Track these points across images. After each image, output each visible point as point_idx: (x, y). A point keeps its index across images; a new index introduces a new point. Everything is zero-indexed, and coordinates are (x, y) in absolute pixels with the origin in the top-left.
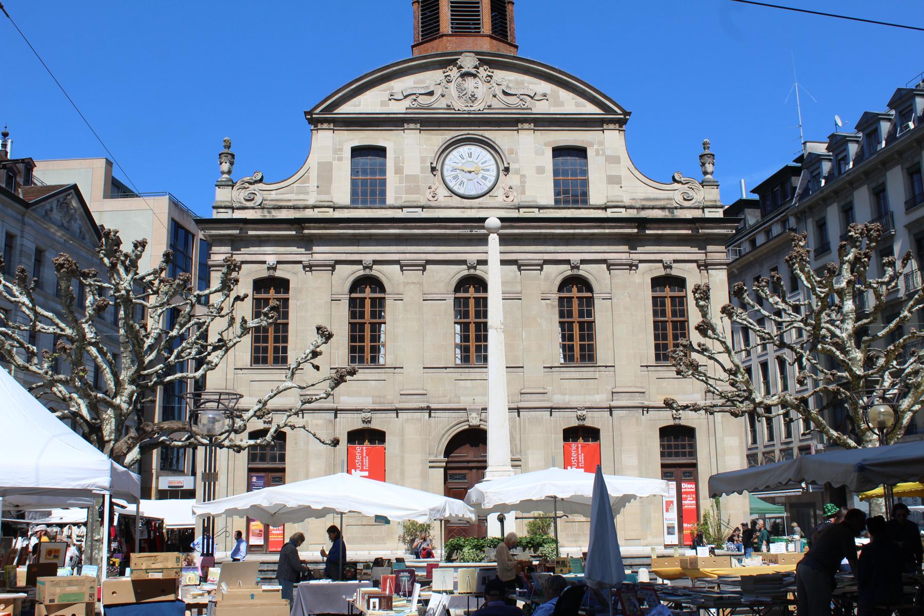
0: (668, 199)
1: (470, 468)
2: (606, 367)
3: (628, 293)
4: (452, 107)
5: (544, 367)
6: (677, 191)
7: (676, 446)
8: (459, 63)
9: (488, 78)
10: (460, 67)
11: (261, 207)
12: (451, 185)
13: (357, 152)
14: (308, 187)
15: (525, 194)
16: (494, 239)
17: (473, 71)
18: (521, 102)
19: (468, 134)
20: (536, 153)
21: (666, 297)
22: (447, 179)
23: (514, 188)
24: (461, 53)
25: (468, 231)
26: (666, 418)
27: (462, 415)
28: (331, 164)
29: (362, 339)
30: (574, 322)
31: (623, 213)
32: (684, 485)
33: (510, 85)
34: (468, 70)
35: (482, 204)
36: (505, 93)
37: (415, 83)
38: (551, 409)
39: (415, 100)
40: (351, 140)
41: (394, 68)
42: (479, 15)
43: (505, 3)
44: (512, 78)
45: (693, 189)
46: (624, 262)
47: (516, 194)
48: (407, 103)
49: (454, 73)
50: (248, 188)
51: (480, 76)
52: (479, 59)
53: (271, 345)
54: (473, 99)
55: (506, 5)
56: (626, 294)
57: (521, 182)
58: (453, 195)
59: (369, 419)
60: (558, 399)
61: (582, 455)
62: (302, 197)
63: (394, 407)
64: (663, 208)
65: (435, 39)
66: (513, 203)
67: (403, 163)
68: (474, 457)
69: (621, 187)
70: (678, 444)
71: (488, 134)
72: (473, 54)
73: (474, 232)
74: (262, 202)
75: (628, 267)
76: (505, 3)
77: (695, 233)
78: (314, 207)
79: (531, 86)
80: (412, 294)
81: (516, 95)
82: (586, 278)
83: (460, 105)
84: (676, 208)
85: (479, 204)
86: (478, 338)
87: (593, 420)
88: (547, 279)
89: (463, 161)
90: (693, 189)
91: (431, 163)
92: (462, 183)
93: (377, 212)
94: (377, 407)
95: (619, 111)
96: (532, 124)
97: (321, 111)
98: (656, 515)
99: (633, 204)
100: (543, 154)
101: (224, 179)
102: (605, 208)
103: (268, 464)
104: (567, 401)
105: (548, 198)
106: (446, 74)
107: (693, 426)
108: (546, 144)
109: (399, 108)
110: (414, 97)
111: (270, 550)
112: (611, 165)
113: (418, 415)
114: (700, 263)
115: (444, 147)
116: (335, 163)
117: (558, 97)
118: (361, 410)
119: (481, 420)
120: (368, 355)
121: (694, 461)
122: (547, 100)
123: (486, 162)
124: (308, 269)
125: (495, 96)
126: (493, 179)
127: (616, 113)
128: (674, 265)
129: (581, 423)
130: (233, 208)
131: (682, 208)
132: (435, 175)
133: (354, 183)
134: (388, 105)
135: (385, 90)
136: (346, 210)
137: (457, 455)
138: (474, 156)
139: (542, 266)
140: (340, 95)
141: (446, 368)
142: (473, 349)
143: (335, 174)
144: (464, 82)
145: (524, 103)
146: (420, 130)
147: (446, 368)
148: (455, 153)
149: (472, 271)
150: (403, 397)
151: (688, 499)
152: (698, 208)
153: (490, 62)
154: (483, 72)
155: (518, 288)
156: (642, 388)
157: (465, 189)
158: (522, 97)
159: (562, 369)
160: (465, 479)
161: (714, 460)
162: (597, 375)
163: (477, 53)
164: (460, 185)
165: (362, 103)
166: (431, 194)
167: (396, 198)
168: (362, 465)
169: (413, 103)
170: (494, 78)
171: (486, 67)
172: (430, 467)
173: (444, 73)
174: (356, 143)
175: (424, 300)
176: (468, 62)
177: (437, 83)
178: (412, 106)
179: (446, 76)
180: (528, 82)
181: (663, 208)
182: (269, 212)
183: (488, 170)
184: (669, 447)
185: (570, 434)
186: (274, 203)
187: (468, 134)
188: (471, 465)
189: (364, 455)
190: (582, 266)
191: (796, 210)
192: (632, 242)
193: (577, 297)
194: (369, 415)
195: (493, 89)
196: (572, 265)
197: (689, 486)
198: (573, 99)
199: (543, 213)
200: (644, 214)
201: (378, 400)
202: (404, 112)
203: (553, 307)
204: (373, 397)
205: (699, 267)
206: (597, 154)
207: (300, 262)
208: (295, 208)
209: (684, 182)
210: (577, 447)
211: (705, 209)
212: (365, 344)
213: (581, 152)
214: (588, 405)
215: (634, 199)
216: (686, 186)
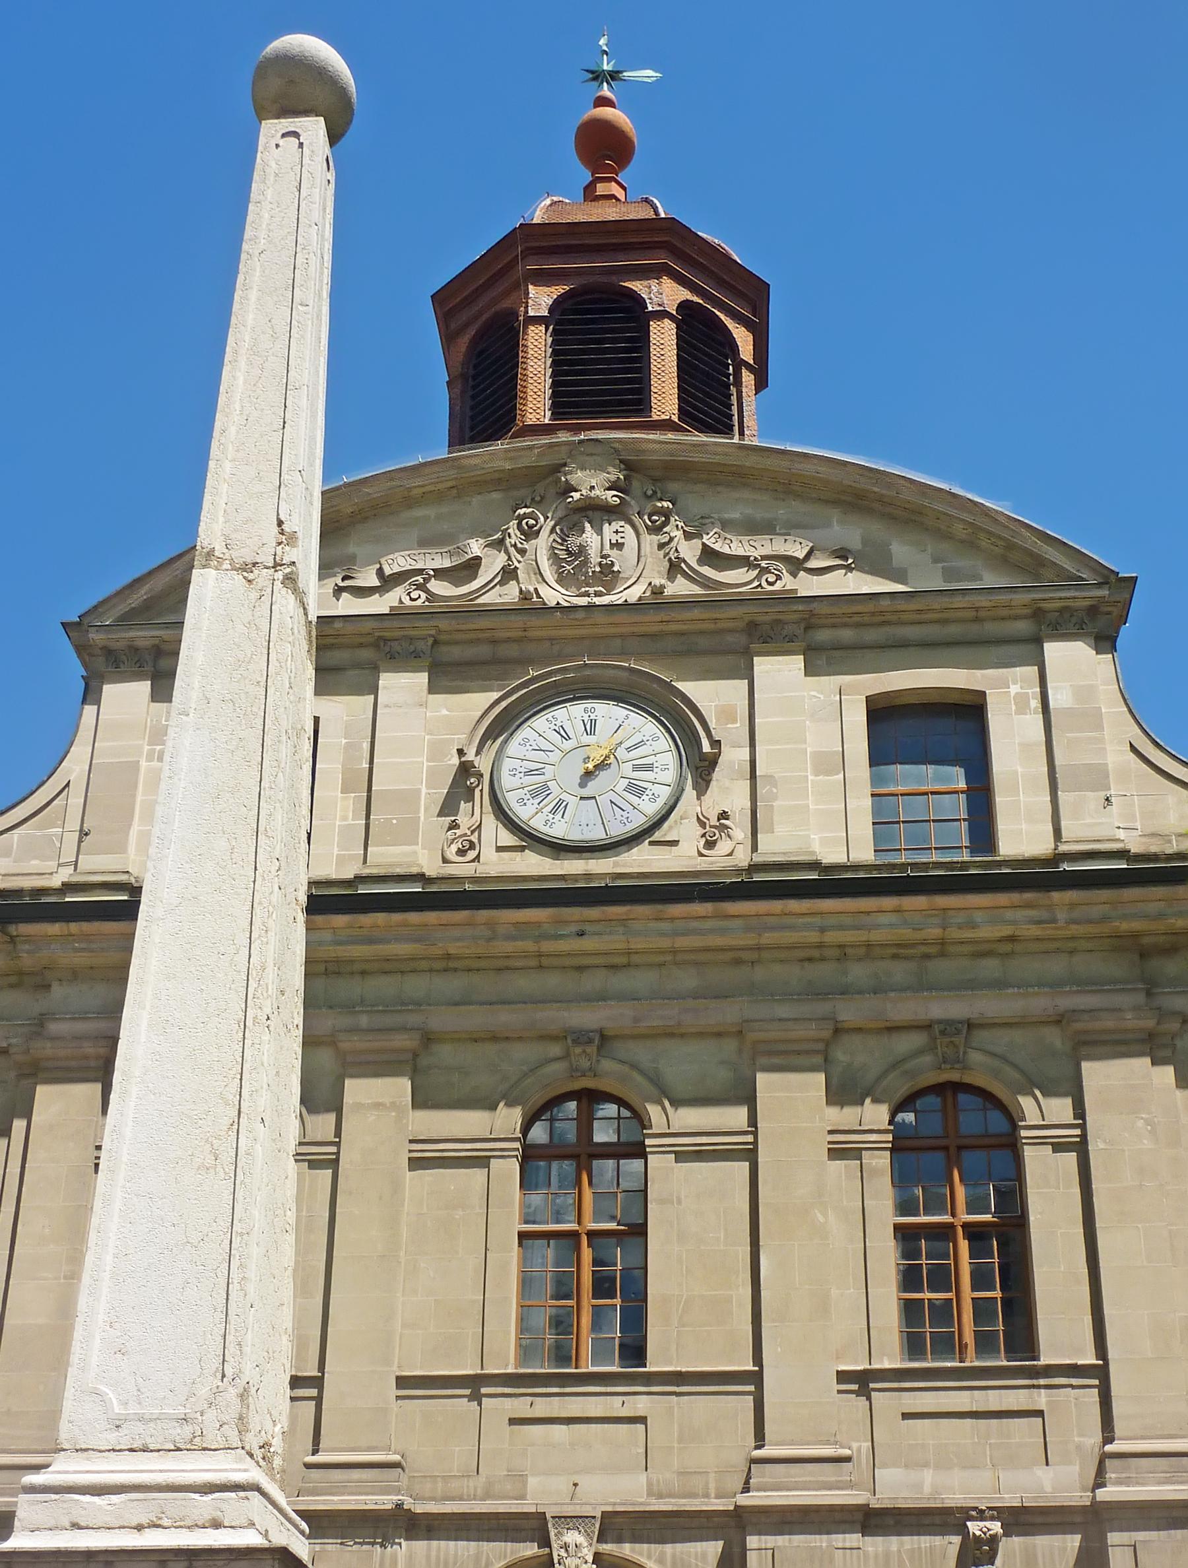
3: (1148, 1122)
15: (773, 832)
22: (512, 800)
56: (1140, 1123)
89: (567, 745)
91: (461, 752)
104: (927, 1490)
126: (664, 793)
158: (764, 564)
162: (1041, 1399)
164: (554, 811)
169: (414, 595)
195: (673, 544)
215: (1153, 835)
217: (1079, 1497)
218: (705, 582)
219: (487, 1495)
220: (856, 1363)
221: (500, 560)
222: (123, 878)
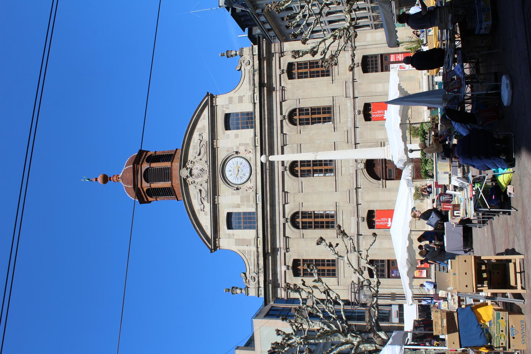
0: (249, 72)
1: (386, 167)
2: (333, 101)
3: (296, 91)
4: (207, 180)
5: (334, 132)
7: (372, 64)
8: (185, 177)
9: (192, 163)
10: (187, 177)
11: (258, 273)
12: (245, 180)
13: (230, 227)
14: (247, 250)
15: (248, 144)
16: (271, 158)
17: (189, 170)
18: (204, 147)
19: (220, 172)
20: (228, 138)
21: (298, 72)
22: (242, 182)
23: (246, 149)
24: (180, 177)
25: (268, 171)
26: (358, 70)
27: (359, 172)
28: (236, 239)
29: (322, 223)
30: (311, 117)
31: (257, 94)
32: (392, 60)
33: (195, 152)
34: (189, 173)
36: (199, 154)
37: (195, 199)
38: (355, 127)
39: (204, 199)
41: (189, 209)
42: (162, 168)
43: (156, 156)
44: (192, 151)
45: (244, 61)
46: (281, 93)
47: (249, 148)
48: (205, 202)
49: (190, 180)
50: (248, 280)
51: (191, 167)
52: (183, 167)
53: (326, 268)
54: (202, 170)
55: (156, 155)
57: (243, 145)
59: (362, 218)
60: (350, 125)
61: (378, 111)
62: (252, 253)
63: (356, 206)
64: (254, 75)
65: (174, 189)
68: (380, 165)
69: (244, 96)
70: (371, 64)
71: (220, 163)
72: (181, 171)
73: (268, 168)
74: (255, 273)
75: (283, 91)
76: (156, 156)
77: (266, 59)
78: (257, 247)
79: (196, 142)
80: (300, 198)
81: (200, 149)
82: (289, 112)
83: (206, 177)
84: (254, 68)
85: (254, 166)
86: (321, 165)
87: (360, 107)
88: (290, 131)
89: (233, 174)
90: (244, 61)
91: (235, 190)
92: (244, 175)
93: (259, 216)
94: (356, 214)
96: (214, 141)
97: (210, 245)
98: (407, 73)
99: (252, 90)
100: (228, 135)
101: (245, 292)
102: (255, 103)
103: (385, 268)
104: (351, 120)
105: (249, 133)
106: (191, 184)
108: (224, 133)
109: (208, 207)
110: (202, 199)
111: (429, 266)
112: (233, 101)
113: (360, 194)
114: (280, 56)
115: (226, 184)
116: (235, 237)
118: (358, 222)
119: (362, 163)
120: (330, 220)
121: (379, 55)
122: (202, 134)
123: (233, 163)
124: (288, 250)
125: (201, 160)
126: (242, 159)
128: (282, 68)
129: (362, 112)
130: (259, 287)
132: (240, 188)
133: (245, 228)
135: (199, 213)
136: (259, 232)
137: (379, 174)
139: (284, 134)
140: (202, 235)
141: (336, 181)
142: (326, 167)
144: (194, 175)
145: (204, 145)
146: (218, 196)
147: (336, 181)
148: (229, 179)
149: (287, 169)
151: (398, 58)
152: (253, 57)
154: (189, 166)
155: (295, 145)
156: (343, 83)
157: (247, 173)
158: (201, 146)
160: (391, 170)
161: (379, 46)
162: (338, 105)
163: (180, 169)
164: (245, 175)
166: (250, 189)
167: (252, 207)
168: (385, 221)
169: (205, 199)
171: (187, 164)
172: (386, 187)
173: (190, 185)
174: (226, 227)
175: (302, 192)
176: (185, 173)
177: (195, 188)
178: (207, 200)
179: (192, 184)
180: (194, 143)
181: (254, 75)
182: (260, 269)
183: (237, 162)
184: (372, 68)
185: (367, 117)
186: (256, 267)
187: (220, 172)
188: (384, 167)
189: (380, 220)
190: (284, 114)
191: (253, 9)
192: (271, 90)
193: (299, 116)
194: (360, 218)
195: (197, 160)
196: (283, 119)
197: (392, 57)
198: (201, 121)
199: (258, 134)
203: (304, 128)
204: (351, 216)
205: (282, 56)
206: (228, 108)
207: (285, 254)
208: (258, 257)
209: (241, 65)
210: (374, 114)
211: (254, 54)
212: (325, 221)
213: (227, 117)
214: (352, 109)
216: (242, 64)
218: (204, 155)
220: (333, 130)
222: (255, 239)
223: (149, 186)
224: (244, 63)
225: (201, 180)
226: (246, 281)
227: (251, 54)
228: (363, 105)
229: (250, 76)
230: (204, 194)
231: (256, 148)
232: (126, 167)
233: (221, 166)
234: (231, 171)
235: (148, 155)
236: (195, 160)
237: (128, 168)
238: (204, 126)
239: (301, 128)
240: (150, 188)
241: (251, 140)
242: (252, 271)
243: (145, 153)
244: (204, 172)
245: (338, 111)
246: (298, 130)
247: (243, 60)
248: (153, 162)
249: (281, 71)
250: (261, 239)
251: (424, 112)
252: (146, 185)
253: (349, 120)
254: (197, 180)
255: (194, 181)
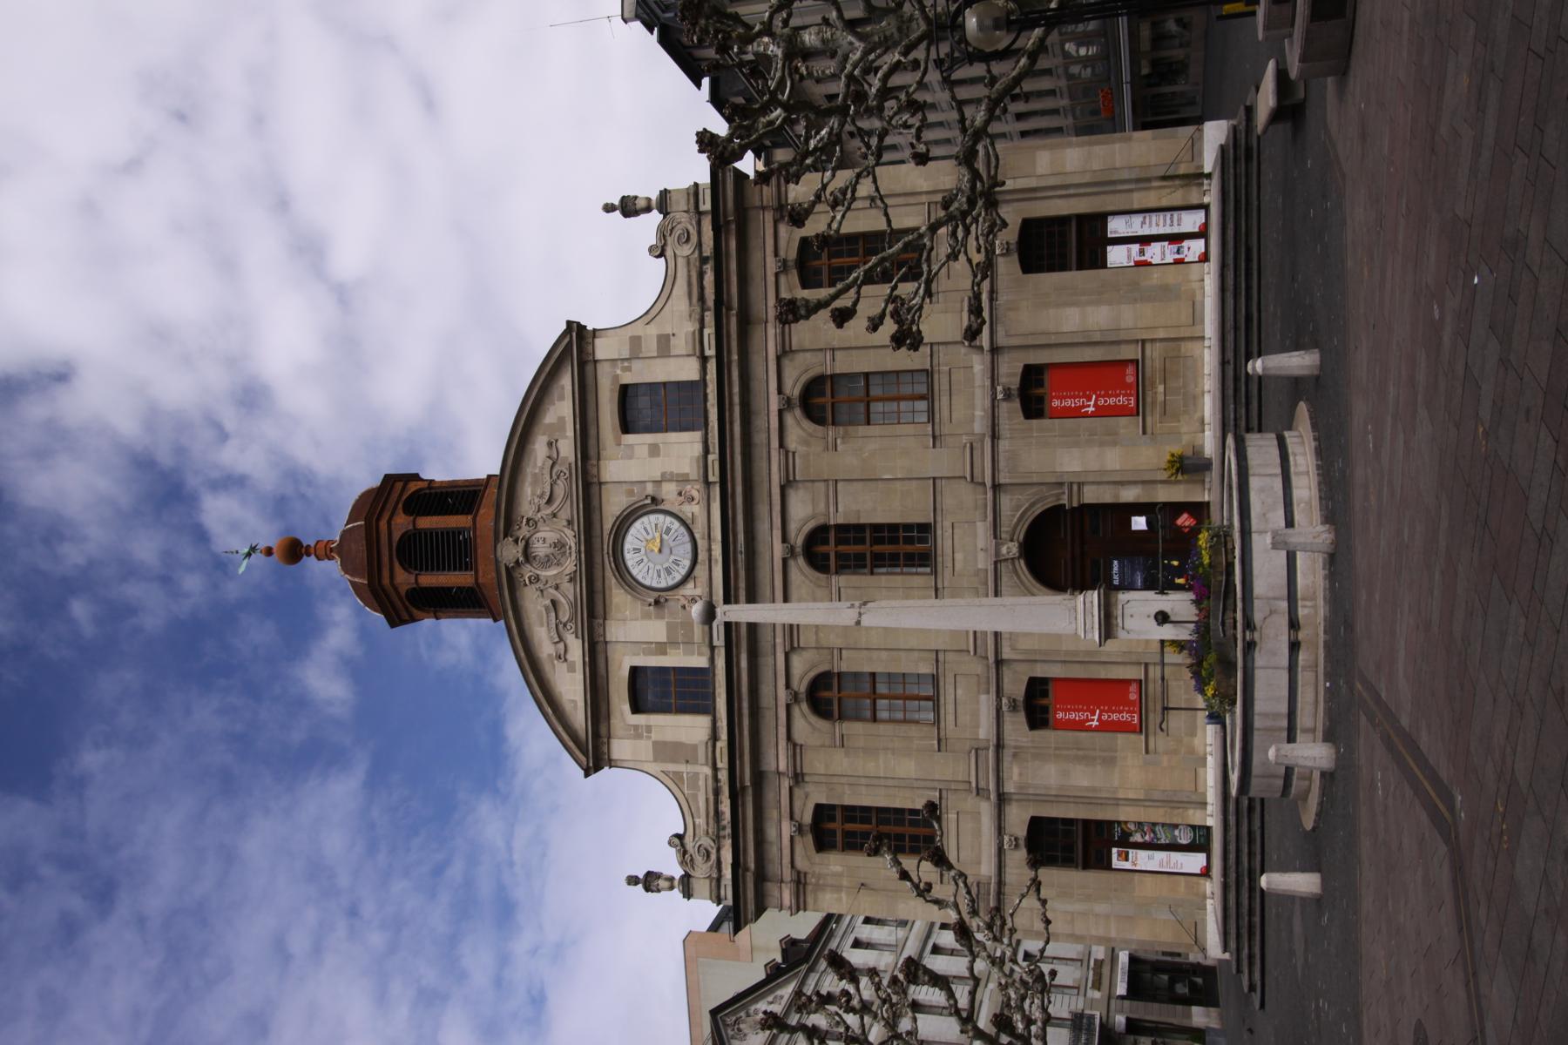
4: (572, 575)
6: (676, 252)
8: (512, 565)
9: (531, 525)
10: (517, 562)
11: (718, 839)
12: (678, 578)
17: (521, 544)
18: (562, 478)
19: (608, 553)
20: (631, 457)
22: (671, 583)
24: (497, 562)
28: (655, 744)
31: (709, 331)
33: (539, 492)
35: (704, 534)
36: (549, 502)
37: (542, 625)
40: (622, 714)
45: (673, 228)
49: (527, 571)
50: (691, 856)
51: (528, 535)
52: (506, 536)
53: (908, 830)
57: (670, 481)
58: (692, 575)
60: (980, 426)
62: (701, 783)
64: (701, 275)
66: (702, 490)
67: (652, 643)
69: (674, 335)
71: (608, 525)
72: (499, 546)
74: (711, 839)
78: (715, 769)
79: (539, 464)
81: (551, 485)
82: (804, 385)
83: (570, 565)
84: (701, 252)
85: (703, 538)
87: (1010, 371)
88: (806, 443)
89: (645, 560)
90: (673, 228)
91: (650, 605)
92: (676, 562)
93: (719, 682)
95: (567, 340)
97: (584, 754)
98: (1155, 276)
104: (983, 413)
106: (527, 582)
107: (1020, 221)
110: (561, 626)
112: (643, 350)
114: (778, 216)
116: (655, 736)
117: (551, 425)
119: (1012, 540)
122: (557, 441)
123: (645, 529)
124: (800, 779)
125: (554, 515)
126: (669, 519)
127: (570, 342)
131: (700, 244)
132: (666, 600)
134: (574, 662)
135: (554, 665)
136: (719, 724)
138: (638, 544)
142: (909, 548)
143: (669, 737)
145: (562, 474)
150: (978, 650)
153: (508, 522)
154: (524, 532)
156: (962, 301)
158: (555, 477)
159: (937, 420)
164: (678, 565)
165: (572, 698)
167: (700, 654)
169: (569, 628)
170: (530, 515)
173: (526, 585)
174: (627, 707)
176: (509, 552)
179: (530, 582)
181: (701, 275)
182: (724, 828)
186: (711, 821)
187: (608, 553)
194: (1004, 701)
195: (544, 517)
196: (786, 406)
198: (554, 404)
199: (714, 448)
200: (710, 302)
201: (983, 686)
202: (580, 641)
204: (979, 692)
206: (629, 369)
207: (791, 789)
211: (701, 209)
214: (988, 383)
215: (690, 316)
216: (669, 240)
217: (988, 357)
219: (986, 584)
221: (552, 591)
223: (413, 581)
224: (673, 236)
225: (555, 572)
226: (684, 857)
227: (692, 209)
228: (1021, 370)
229: (689, 277)
230: (565, 615)
231: (709, 488)
232: (349, 526)
233: (612, 536)
234: (639, 550)
235: (411, 492)
236: (539, 515)
237: (354, 527)
238: (562, 419)
239: (839, 433)
240: (415, 586)
241: (695, 465)
242: (701, 831)
243: (399, 485)
244: (566, 552)
245: (945, 387)
246: (830, 439)
247: (670, 227)
248: (423, 515)
249: (780, 264)
250: (722, 744)
251: (1203, 395)
252: (404, 579)
253: (979, 413)
254: (544, 574)
255: (538, 575)
